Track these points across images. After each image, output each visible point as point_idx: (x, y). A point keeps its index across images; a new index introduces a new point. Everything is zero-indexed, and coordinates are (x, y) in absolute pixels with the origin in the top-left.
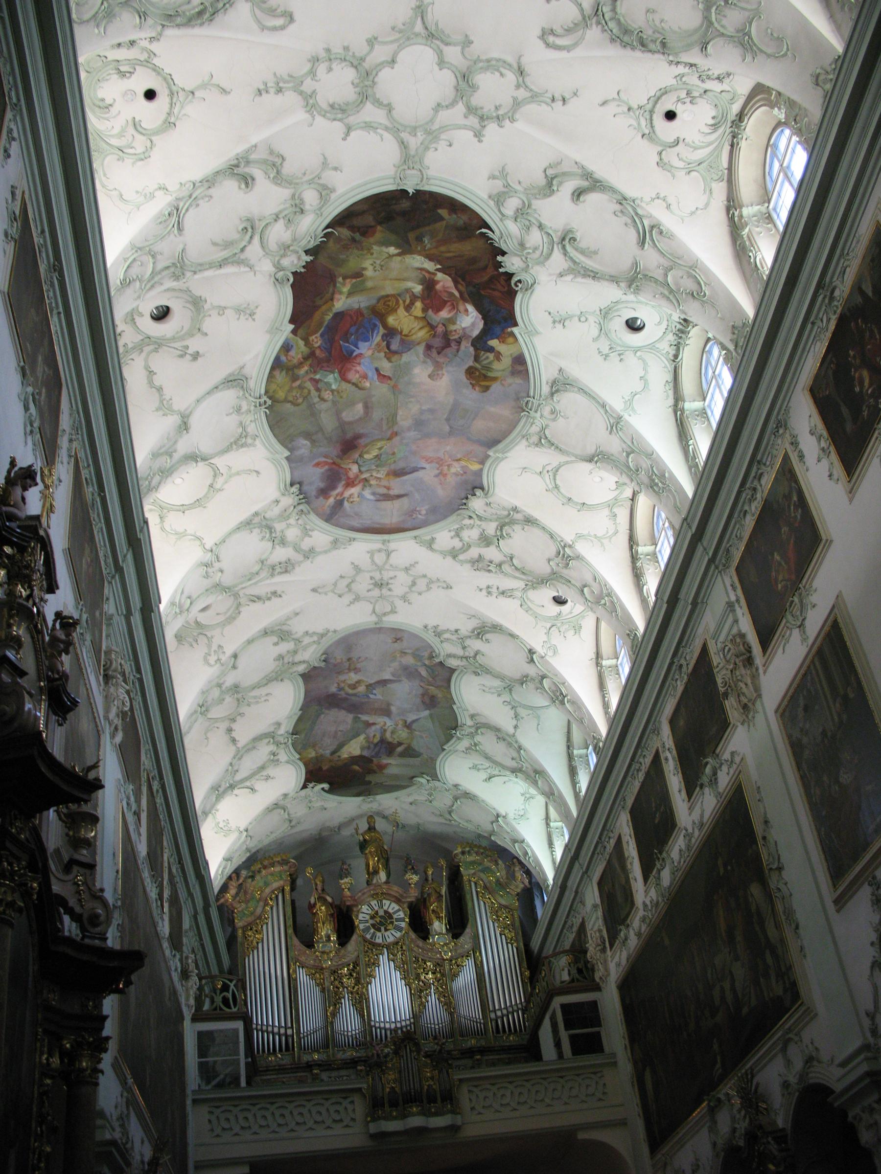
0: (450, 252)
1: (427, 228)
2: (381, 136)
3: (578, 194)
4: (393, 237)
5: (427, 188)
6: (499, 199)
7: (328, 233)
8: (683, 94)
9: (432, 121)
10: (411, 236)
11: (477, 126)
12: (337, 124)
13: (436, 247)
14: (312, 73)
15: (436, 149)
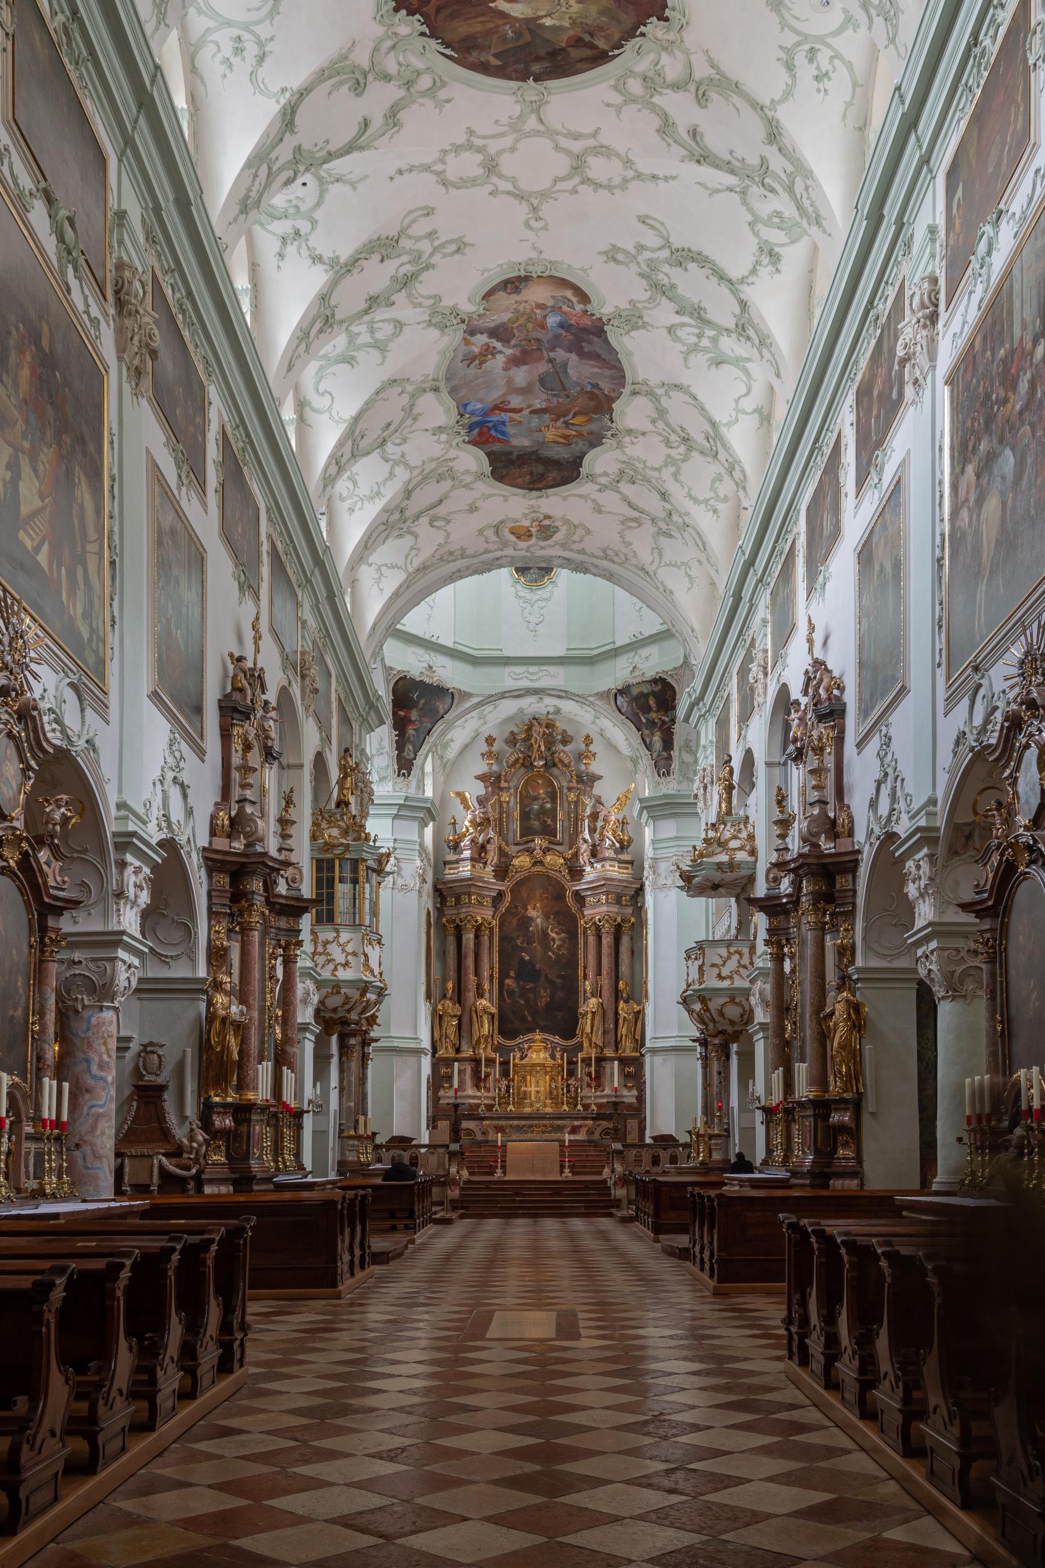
0: (482, 22)
1: (511, 46)
2: (564, 127)
3: (366, 124)
4: (547, 35)
5: (514, 84)
6: (438, 84)
7: (618, 49)
8: (304, 208)
9: (517, 141)
10: (527, 38)
11: (473, 139)
12: (605, 143)
13: (497, 26)
14: (625, 180)
15: (510, 118)
